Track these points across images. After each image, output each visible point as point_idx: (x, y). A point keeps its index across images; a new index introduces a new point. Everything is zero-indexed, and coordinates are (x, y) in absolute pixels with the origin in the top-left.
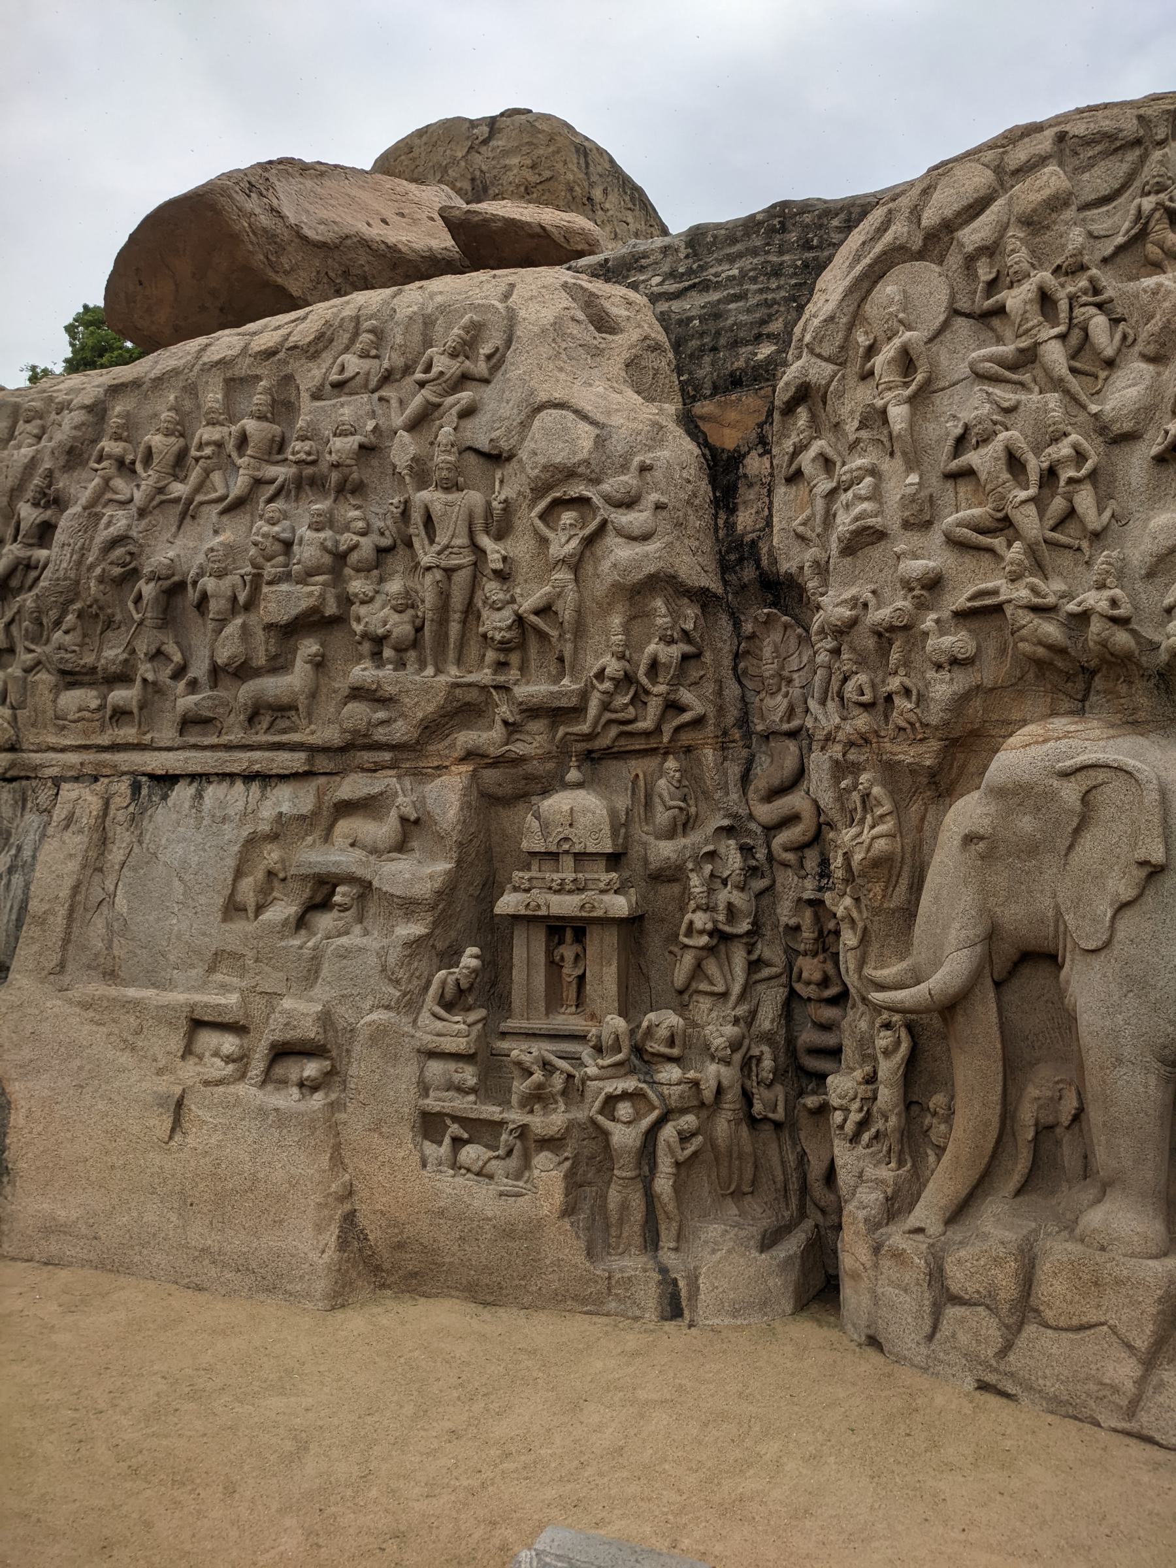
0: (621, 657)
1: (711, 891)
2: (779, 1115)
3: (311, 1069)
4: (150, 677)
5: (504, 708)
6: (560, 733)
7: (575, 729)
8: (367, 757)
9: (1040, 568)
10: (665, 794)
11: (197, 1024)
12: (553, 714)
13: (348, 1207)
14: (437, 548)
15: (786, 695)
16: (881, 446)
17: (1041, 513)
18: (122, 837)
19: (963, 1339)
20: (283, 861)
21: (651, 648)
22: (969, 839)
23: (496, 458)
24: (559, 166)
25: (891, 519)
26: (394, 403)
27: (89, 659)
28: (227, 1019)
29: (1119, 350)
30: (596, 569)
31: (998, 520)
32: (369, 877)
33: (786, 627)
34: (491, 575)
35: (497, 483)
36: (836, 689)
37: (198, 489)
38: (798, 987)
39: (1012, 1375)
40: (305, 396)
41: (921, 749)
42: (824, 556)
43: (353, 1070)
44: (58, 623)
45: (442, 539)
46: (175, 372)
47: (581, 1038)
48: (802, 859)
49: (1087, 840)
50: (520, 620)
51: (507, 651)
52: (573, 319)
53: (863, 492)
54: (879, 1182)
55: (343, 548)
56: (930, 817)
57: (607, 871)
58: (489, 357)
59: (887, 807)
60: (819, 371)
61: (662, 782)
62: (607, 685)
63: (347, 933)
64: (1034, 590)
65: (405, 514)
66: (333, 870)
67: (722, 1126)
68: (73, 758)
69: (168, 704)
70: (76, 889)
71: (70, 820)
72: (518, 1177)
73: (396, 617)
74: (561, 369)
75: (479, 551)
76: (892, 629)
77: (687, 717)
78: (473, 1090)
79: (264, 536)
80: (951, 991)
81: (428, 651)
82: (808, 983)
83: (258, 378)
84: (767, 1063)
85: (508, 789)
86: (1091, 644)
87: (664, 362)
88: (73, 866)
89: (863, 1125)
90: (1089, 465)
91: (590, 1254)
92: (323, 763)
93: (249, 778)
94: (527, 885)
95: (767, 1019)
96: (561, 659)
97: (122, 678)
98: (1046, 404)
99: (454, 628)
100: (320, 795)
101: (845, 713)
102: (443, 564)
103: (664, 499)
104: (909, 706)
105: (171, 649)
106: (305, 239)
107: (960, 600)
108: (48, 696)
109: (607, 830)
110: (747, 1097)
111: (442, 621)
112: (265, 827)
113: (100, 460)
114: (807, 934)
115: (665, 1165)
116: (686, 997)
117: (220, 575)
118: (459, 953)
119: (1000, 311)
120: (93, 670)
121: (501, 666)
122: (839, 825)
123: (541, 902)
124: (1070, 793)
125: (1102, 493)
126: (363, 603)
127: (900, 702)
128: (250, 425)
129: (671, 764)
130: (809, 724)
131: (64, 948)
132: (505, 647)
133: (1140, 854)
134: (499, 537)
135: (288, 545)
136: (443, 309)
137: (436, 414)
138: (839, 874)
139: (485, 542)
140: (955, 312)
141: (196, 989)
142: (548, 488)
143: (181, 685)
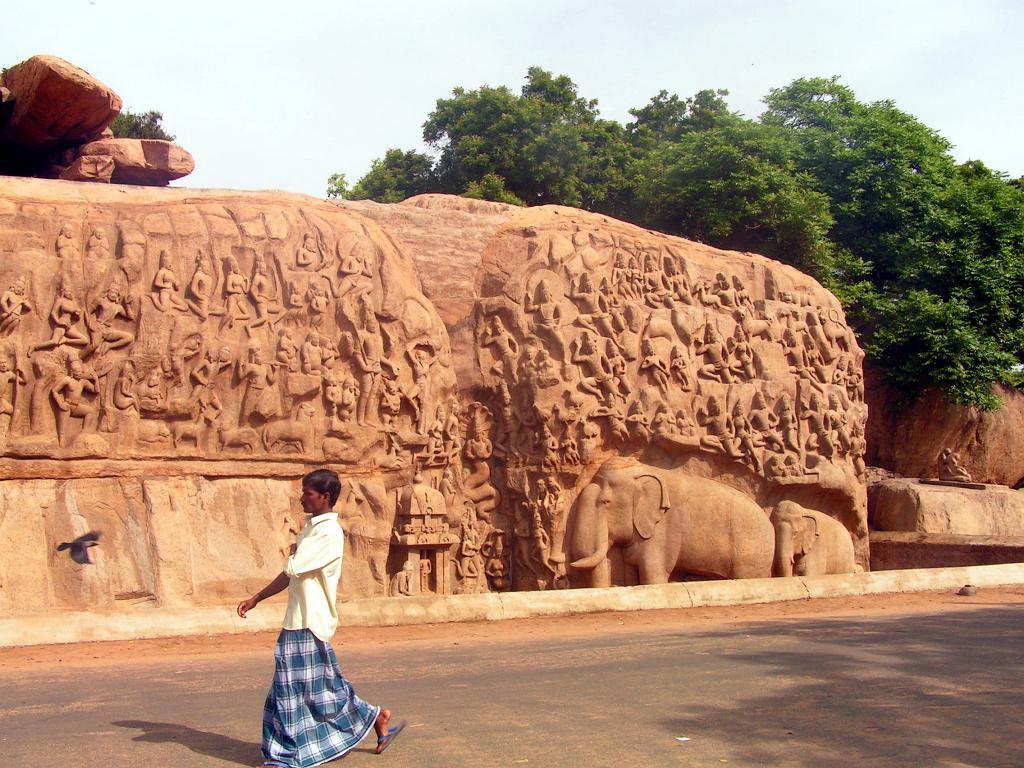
6: (416, 455)
10: (450, 486)
12: (414, 448)
27: (160, 403)
35: (387, 332)
40: (284, 268)
44: (141, 380)
50: (405, 401)
55: (326, 356)
57: (444, 522)
60: (509, 304)
62: (437, 435)
69: (213, 434)
79: (288, 345)
90: (626, 367)
97: (187, 417)
105: (217, 401)
116: (464, 579)
119: (582, 300)
120: (163, 411)
121: (391, 421)
126: (334, 386)
127: (570, 449)
129: (449, 472)
130: (502, 455)
137: (354, 290)
139: (385, 360)
142: (414, 338)
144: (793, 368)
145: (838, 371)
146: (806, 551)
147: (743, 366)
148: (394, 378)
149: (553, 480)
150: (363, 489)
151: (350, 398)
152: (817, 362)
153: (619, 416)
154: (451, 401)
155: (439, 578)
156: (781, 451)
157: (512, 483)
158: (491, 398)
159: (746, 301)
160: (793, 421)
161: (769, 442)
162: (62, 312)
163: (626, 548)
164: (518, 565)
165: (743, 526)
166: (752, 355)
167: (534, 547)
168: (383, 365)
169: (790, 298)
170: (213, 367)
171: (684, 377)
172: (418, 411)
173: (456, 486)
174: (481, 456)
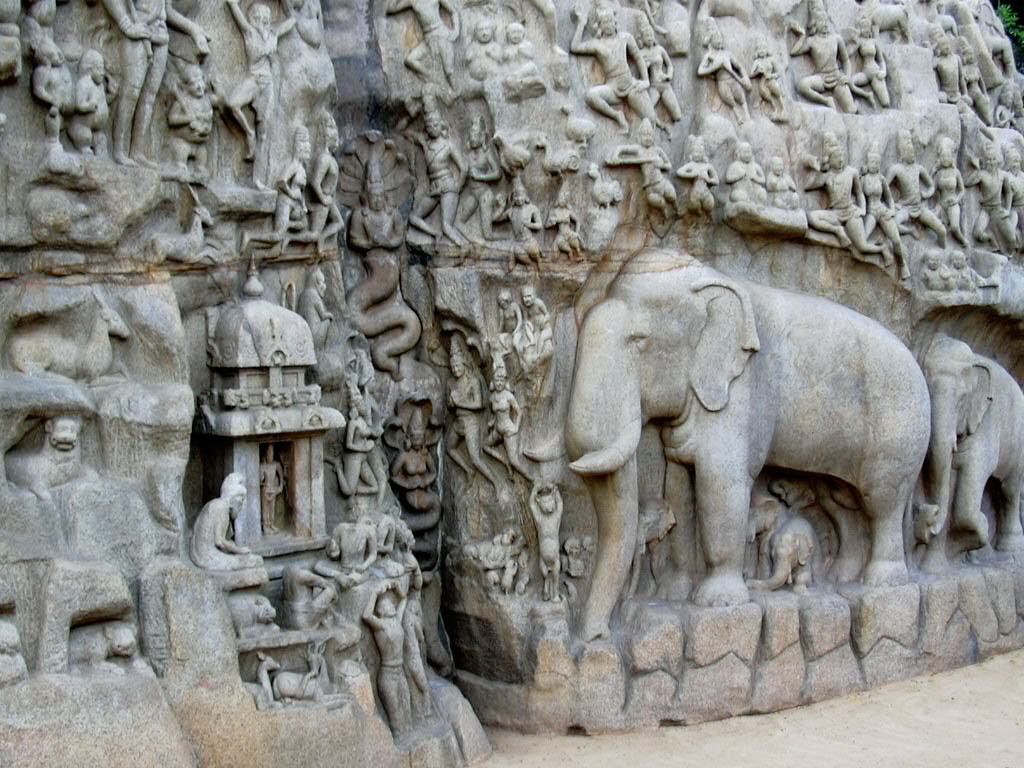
5: (205, 210)
7: (266, 234)
8: (60, 258)
12: (244, 217)
14: (150, 17)
15: (390, 214)
16: (510, 12)
19: (650, 696)
22: (633, 338)
30: (283, 69)
31: (619, 98)
32: (91, 407)
33: (388, 148)
34: (194, 59)
36: (488, 216)
38: (399, 480)
39: (681, 707)
41: (578, 268)
42: (450, 94)
43: (153, 627)
48: (399, 363)
51: (198, 143)
53: (529, 53)
54: (556, 613)
56: (560, 321)
57: (308, 382)
62: (296, 192)
66: (56, 400)
72: (328, 691)
81: (122, 136)
82: (412, 475)
85: (191, 299)
86: (693, 199)
89: (516, 577)
90: (671, 69)
94: (247, 404)
96: (249, 162)
98: (636, 18)
101: (496, 235)
102: (155, 37)
104: (576, 234)
107: (614, 158)
111: (139, 103)
114: (418, 431)
116: (352, 500)
121: (191, 158)
122: (483, 331)
123: (276, 419)
124: (700, 302)
126: (54, 66)
127: (565, 229)
129: (319, 274)
130: (423, 241)
132: (200, 141)
133: (748, 346)
134: (185, 15)
138: (503, 372)
139: (179, 19)
144: (944, 95)
145: (1001, 108)
146: (973, 429)
147: (869, 84)
148: (202, 58)
149: (529, 291)
150: (127, 310)
152: (978, 90)
153: (661, 164)
155: (301, 503)
156: (940, 244)
157: (449, 297)
158: (404, 122)
160: (958, 187)
161: (918, 222)
163: (672, 427)
164: (457, 464)
165: (886, 386)
167: (491, 429)
168: (172, 26)
171: (774, 94)
172: (252, 138)
173: (330, 304)
174: (381, 242)
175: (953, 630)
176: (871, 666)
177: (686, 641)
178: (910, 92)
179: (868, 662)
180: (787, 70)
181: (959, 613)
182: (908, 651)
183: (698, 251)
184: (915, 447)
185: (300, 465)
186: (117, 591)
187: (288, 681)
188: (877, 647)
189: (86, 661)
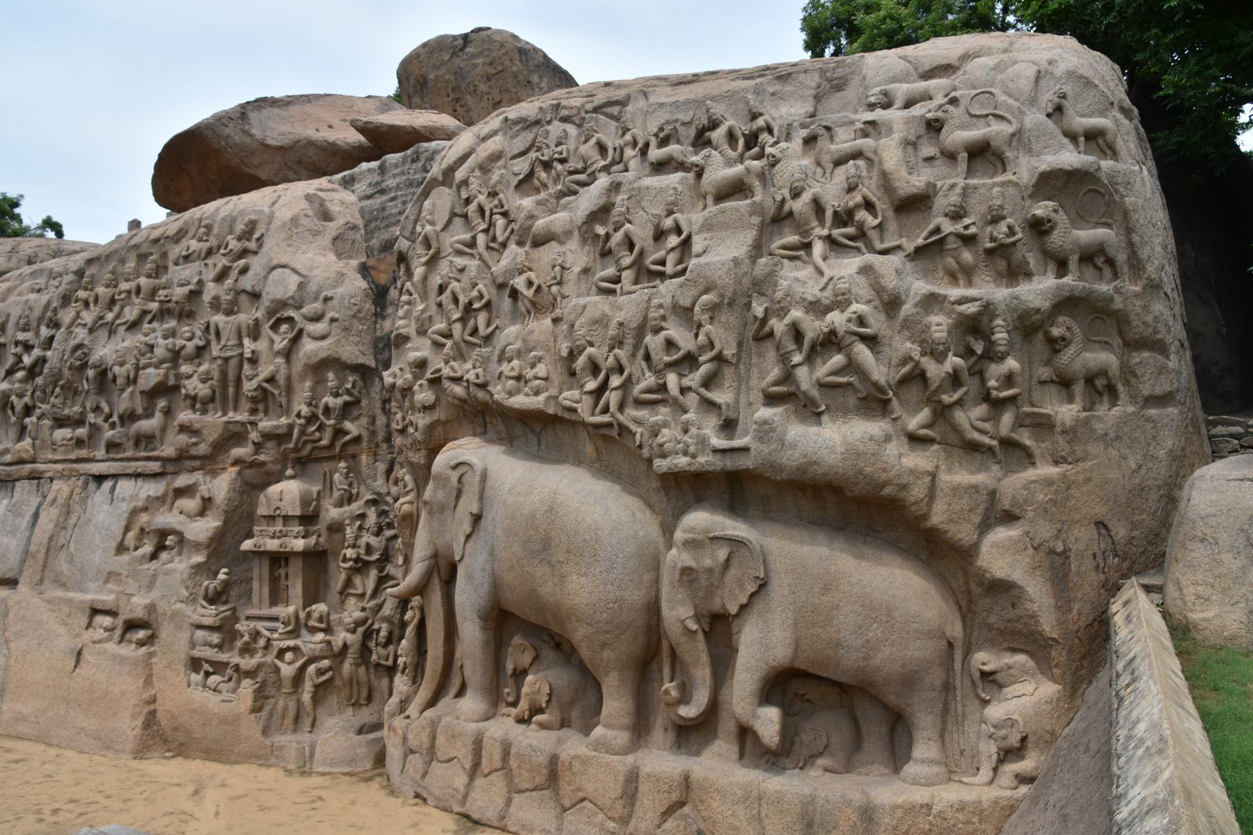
0: (310, 404)
1: (357, 538)
2: (390, 663)
3: (141, 634)
4: (92, 421)
9: (461, 357)
11: (95, 611)
13: (152, 707)
17: (464, 328)
18: (77, 509)
19: (411, 770)
20: (148, 522)
21: (325, 399)
22: (426, 503)
23: (255, 296)
24: (507, 63)
25: (411, 330)
26: (211, 266)
27: (66, 412)
28: (107, 608)
29: (508, 238)
37: (118, 316)
40: (171, 264)
44: (53, 392)
45: (223, 342)
46: (116, 251)
47: (276, 619)
49: (462, 500)
52: (306, 215)
58: (258, 239)
59: (411, 485)
61: (337, 476)
63: (172, 561)
64: (452, 369)
65: (208, 328)
67: (347, 667)
68: (59, 467)
70: (51, 539)
71: (54, 500)
73: (201, 386)
74: (290, 245)
75: (241, 345)
76: (404, 390)
77: (348, 437)
78: (220, 647)
80: (413, 585)
83: (151, 254)
84: (383, 633)
87: (359, 235)
88: (51, 526)
91: (265, 732)
92: (170, 468)
93: (137, 476)
95: (387, 610)
96: (281, 406)
97: (80, 422)
99: (231, 390)
100: (168, 485)
103: (336, 316)
106: (268, 146)
107: (428, 375)
108: (48, 433)
109: (298, 503)
110: (365, 651)
111: (224, 386)
112: (140, 504)
113: (76, 301)
115: (308, 687)
117: (122, 364)
118: (217, 573)
120: (69, 417)
121: (254, 411)
124: (454, 479)
125: (494, 314)
127: (411, 430)
128: (143, 281)
129: (342, 464)
131: (43, 571)
132: (254, 400)
135: (151, 347)
136: (242, 213)
139: (246, 341)
140: (453, 215)
141: (98, 592)
143: (106, 426)
146: (733, 610)
151: (203, 390)
152: (862, 215)
154: (326, 380)
159: (764, 137)
162: (17, 343)
166: (683, 236)
169: (872, 99)
170: (91, 373)
175: (670, 824)
176: (570, 822)
177: (433, 738)
178: (698, 256)
179: (569, 816)
180: (586, 271)
181: (686, 810)
182: (613, 824)
183: (504, 435)
184: (605, 615)
185: (291, 570)
186: (140, 613)
187: (214, 679)
188: (578, 806)
189: (130, 642)
